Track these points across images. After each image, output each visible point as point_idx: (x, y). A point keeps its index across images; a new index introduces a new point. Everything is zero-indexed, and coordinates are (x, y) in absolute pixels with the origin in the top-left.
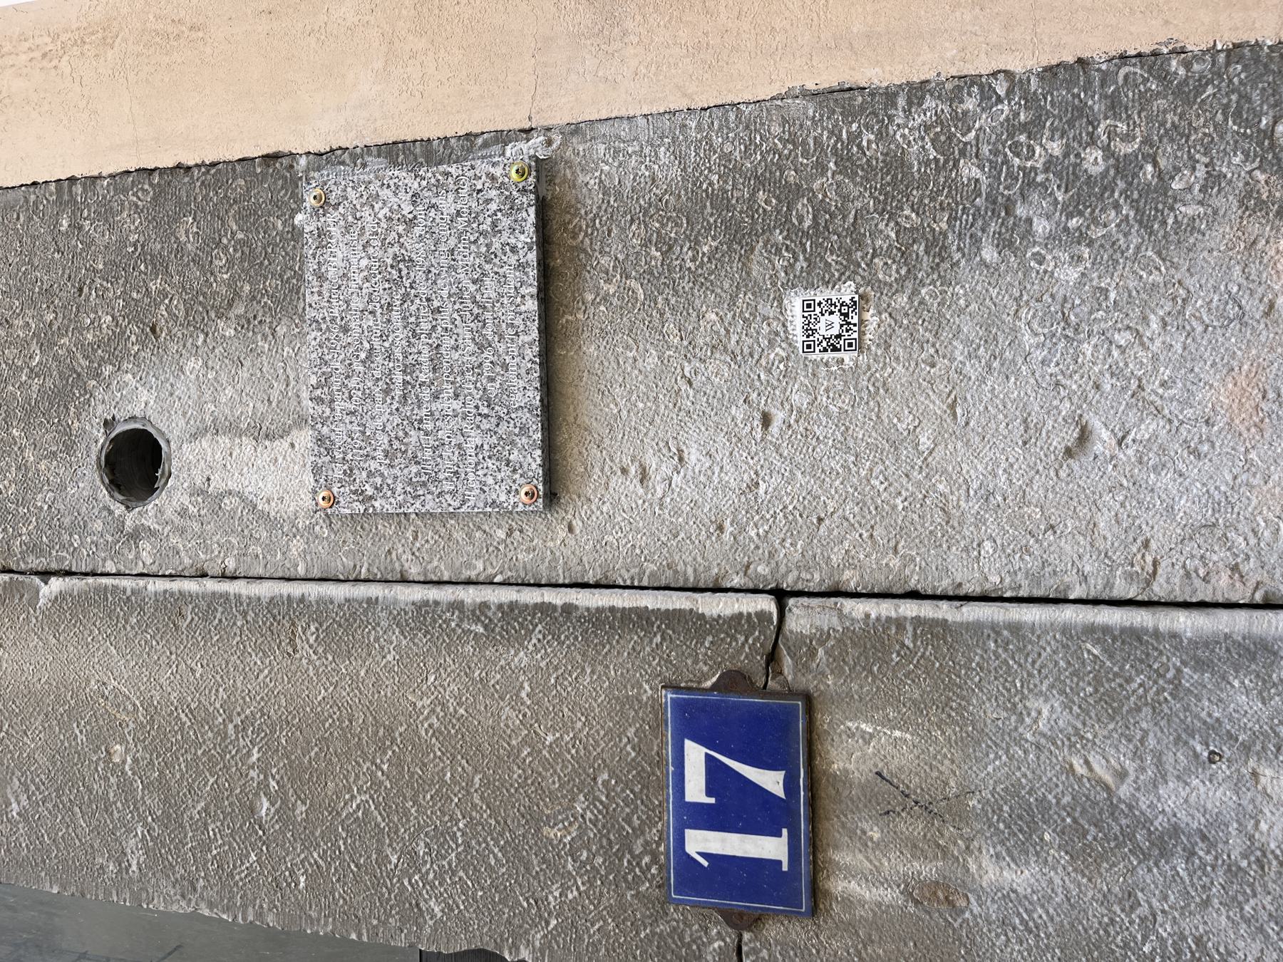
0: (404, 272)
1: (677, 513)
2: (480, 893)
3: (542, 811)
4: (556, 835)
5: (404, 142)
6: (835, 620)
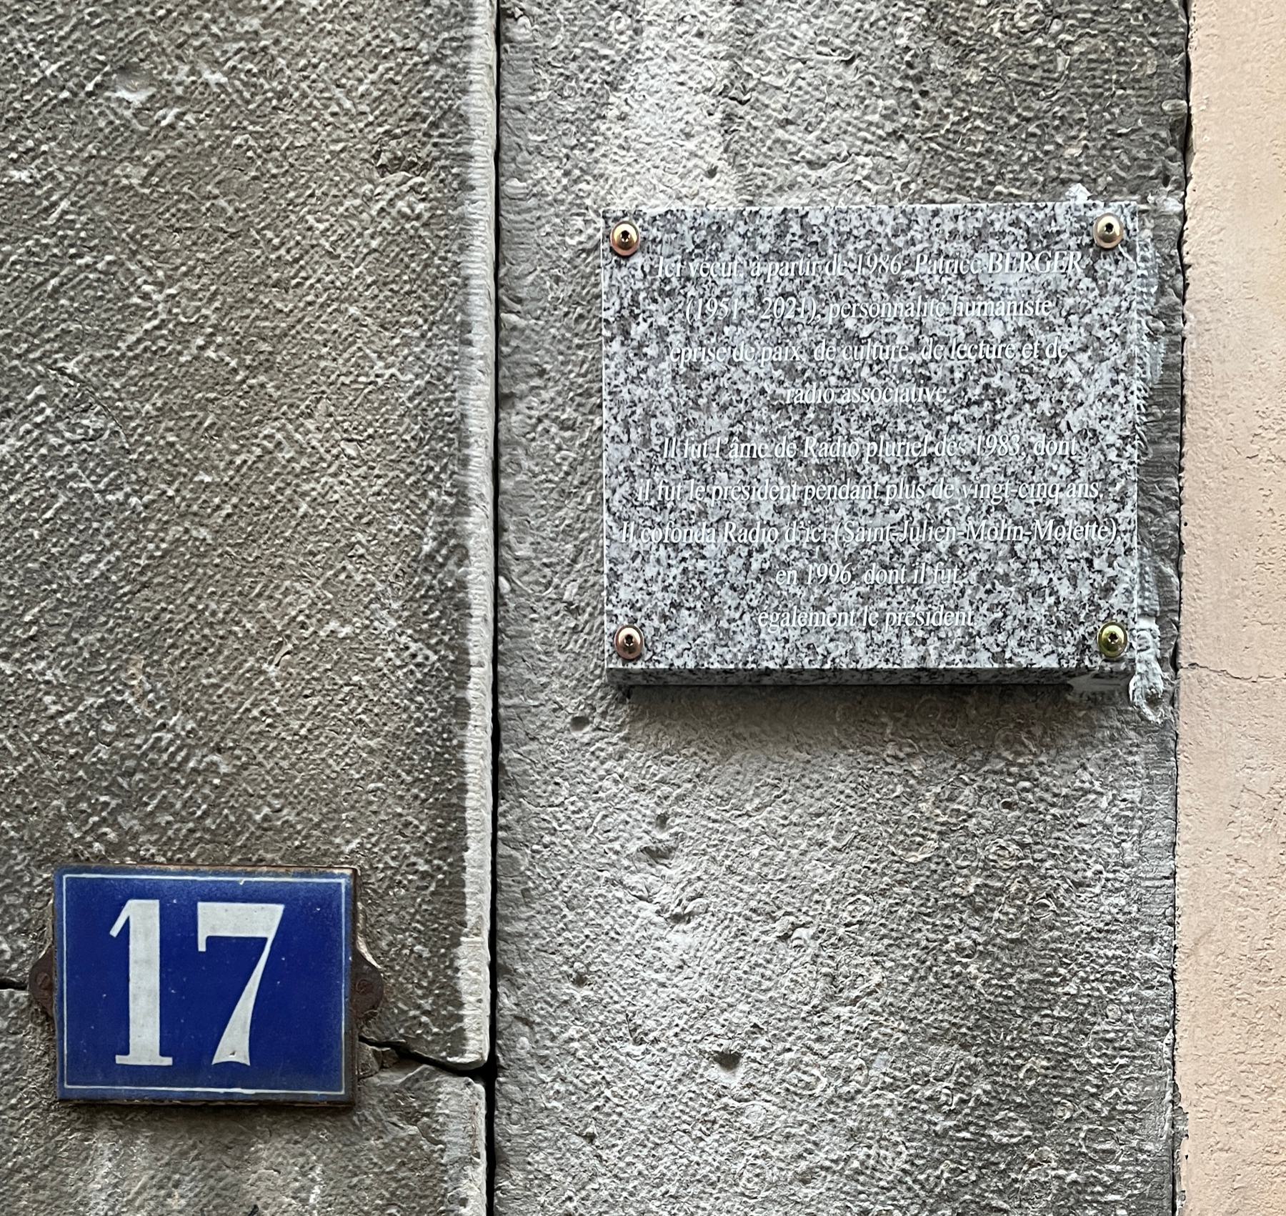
0: (976, 411)
1: (603, 910)
2: (36, 534)
3: (166, 654)
4: (133, 677)
5: (1183, 420)
6: (455, 1153)
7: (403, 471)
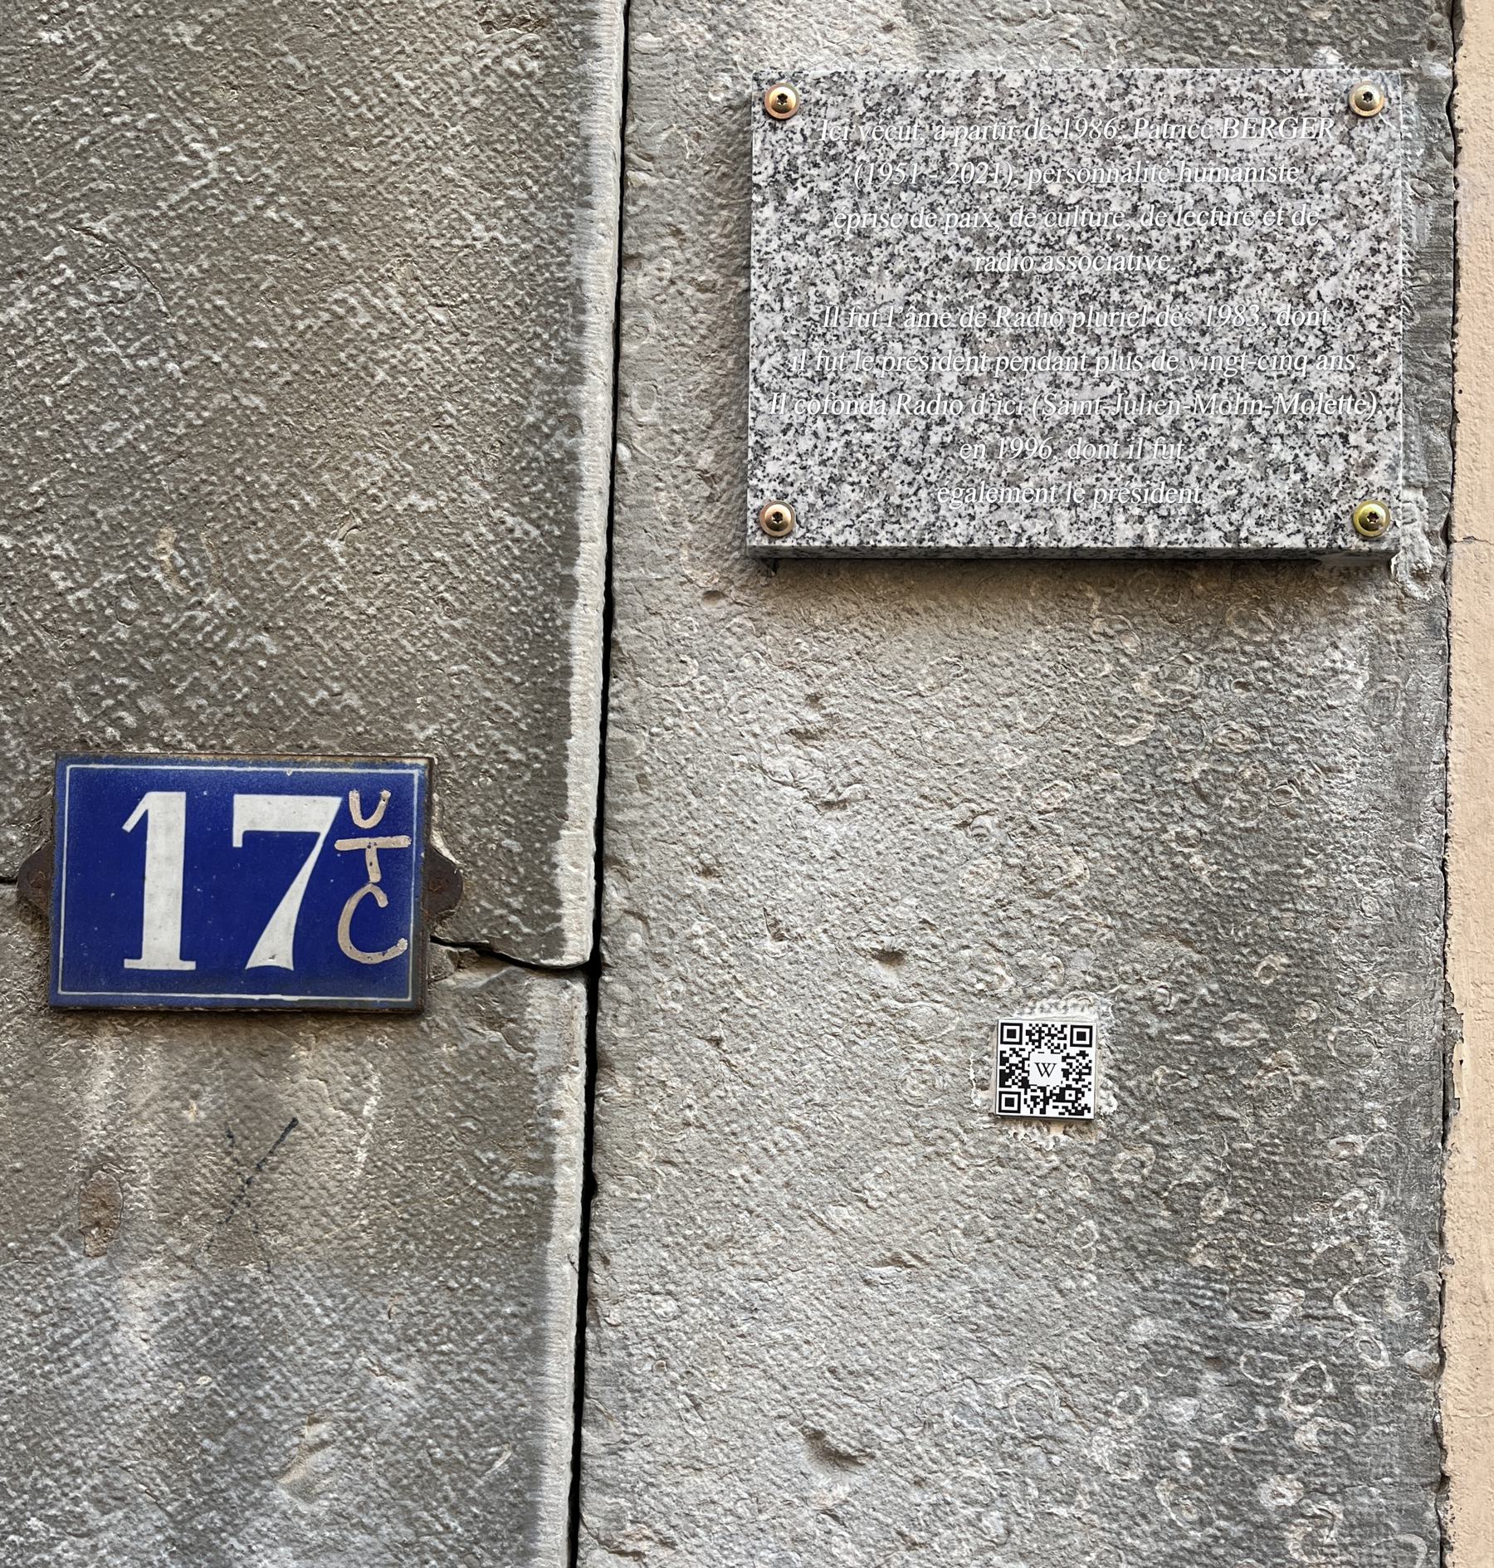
7: (503, 338)
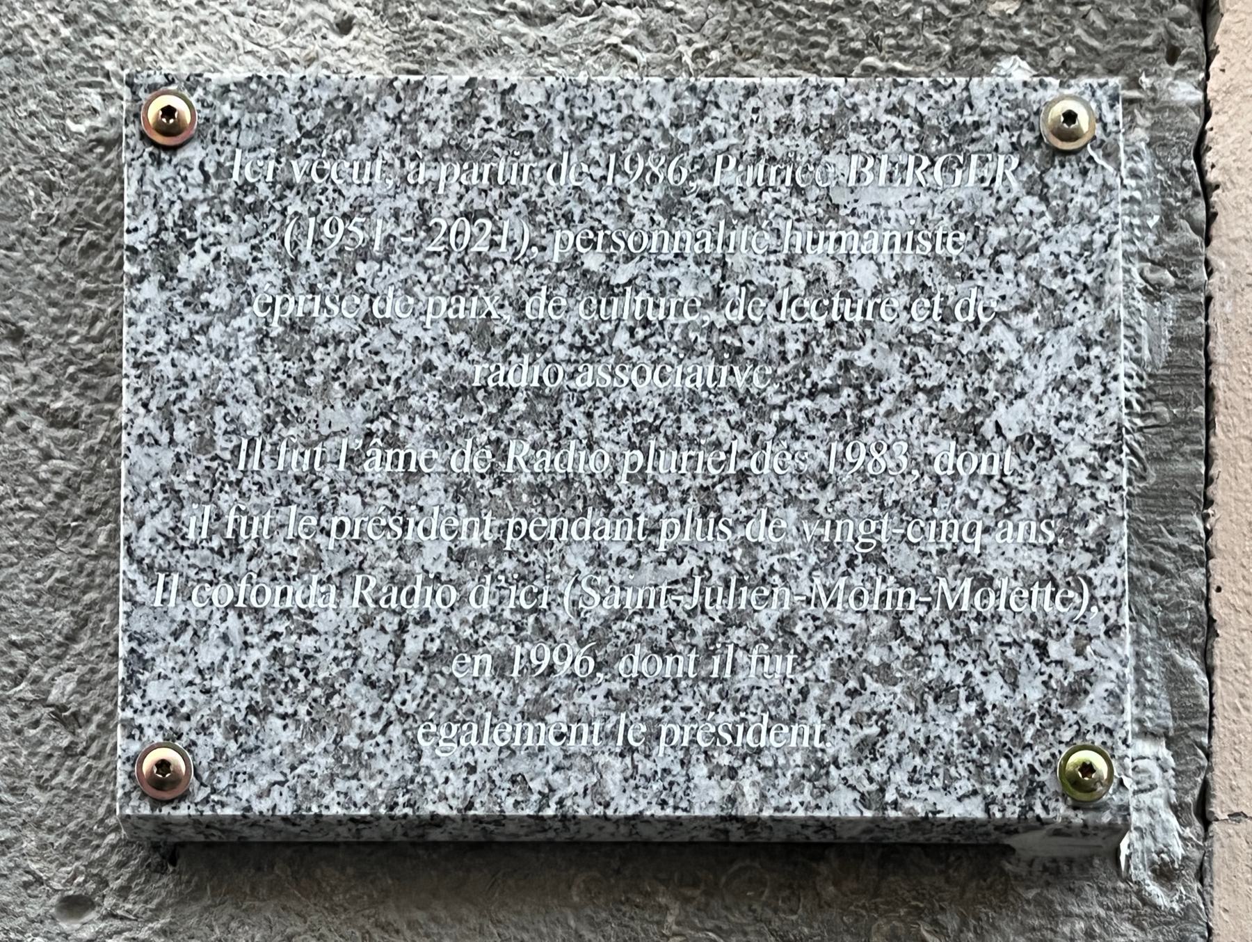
0: (828, 405)
